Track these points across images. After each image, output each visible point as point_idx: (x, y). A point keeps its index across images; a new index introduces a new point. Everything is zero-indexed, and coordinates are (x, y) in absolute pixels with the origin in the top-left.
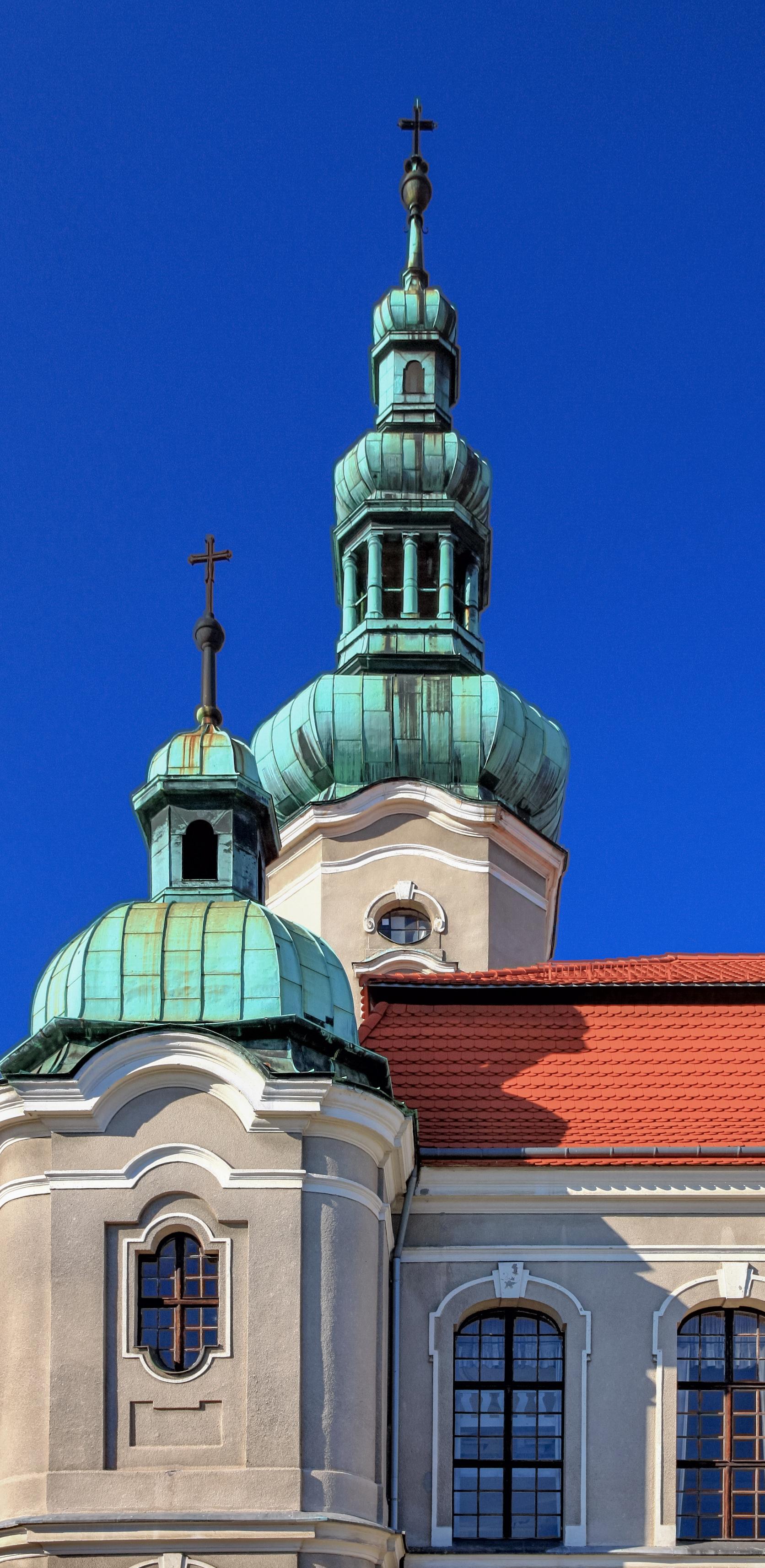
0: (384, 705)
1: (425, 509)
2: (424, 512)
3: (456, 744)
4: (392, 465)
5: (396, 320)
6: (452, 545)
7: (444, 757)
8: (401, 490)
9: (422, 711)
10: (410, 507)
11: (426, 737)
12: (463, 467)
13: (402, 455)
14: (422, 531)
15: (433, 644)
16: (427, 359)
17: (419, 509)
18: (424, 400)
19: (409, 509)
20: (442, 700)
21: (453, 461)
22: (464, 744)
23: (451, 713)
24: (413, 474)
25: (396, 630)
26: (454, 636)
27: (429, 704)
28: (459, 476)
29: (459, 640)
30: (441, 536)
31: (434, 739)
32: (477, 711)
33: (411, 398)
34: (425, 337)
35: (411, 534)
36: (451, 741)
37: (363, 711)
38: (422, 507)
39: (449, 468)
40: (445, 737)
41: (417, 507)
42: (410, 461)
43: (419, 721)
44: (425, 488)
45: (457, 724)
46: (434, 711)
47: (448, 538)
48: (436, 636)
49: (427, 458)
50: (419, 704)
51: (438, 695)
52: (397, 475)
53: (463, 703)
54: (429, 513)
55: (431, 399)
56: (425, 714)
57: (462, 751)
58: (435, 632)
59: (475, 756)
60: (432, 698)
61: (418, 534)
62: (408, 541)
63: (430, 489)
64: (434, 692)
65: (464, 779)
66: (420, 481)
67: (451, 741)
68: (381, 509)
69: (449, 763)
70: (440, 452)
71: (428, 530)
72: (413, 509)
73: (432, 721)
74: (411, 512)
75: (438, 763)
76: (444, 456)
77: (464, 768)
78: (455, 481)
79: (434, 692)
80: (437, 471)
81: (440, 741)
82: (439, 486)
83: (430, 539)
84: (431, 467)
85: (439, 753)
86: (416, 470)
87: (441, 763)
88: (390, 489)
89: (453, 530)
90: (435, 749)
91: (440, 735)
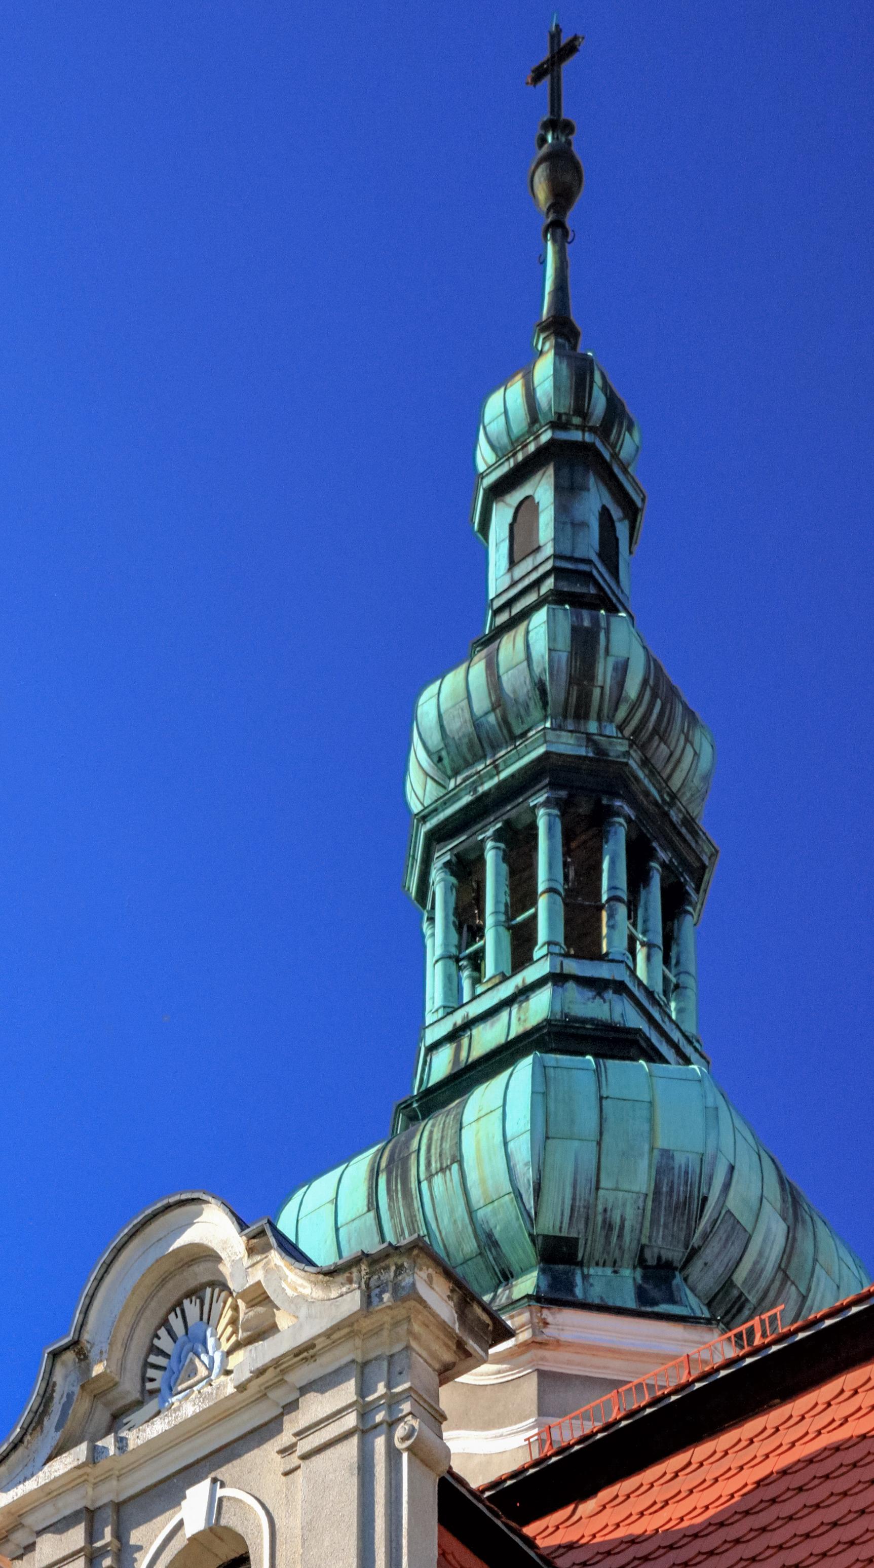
0: (365, 1202)
1: (503, 775)
2: (505, 780)
3: (480, 1214)
4: (458, 725)
5: (495, 443)
6: (556, 812)
7: (470, 1246)
8: (484, 757)
9: (419, 1182)
10: (482, 784)
11: (434, 1226)
12: (564, 656)
13: (469, 697)
14: (505, 817)
15: (523, 1018)
16: (543, 481)
17: (496, 780)
18: (540, 557)
19: (481, 790)
20: (447, 1146)
21: (543, 657)
22: (490, 1207)
23: (460, 1163)
24: (492, 718)
25: (469, 1024)
26: (555, 984)
27: (428, 1164)
28: (564, 677)
29: (571, 985)
30: (535, 806)
31: (445, 1221)
32: (499, 1138)
33: (519, 572)
34: (532, 448)
35: (490, 833)
36: (471, 1212)
37: (337, 1229)
38: (498, 773)
39: (541, 673)
40: (461, 1210)
41: (492, 777)
42: (481, 703)
43: (416, 1204)
44: (518, 731)
45: (472, 1177)
46: (437, 1173)
47: (547, 804)
48: (527, 999)
49: (504, 678)
50: (413, 1172)
51: (442, 1138)
52: (469, 735)
53: (478, 1133)
54: (513, 776)
55: (548, 550)
56: (424, 1185)
57: (492, 1223)
58: (525, 992)
59: (514, 1220)
60: (433, 1151)
61: (499, 825)
62: (489, 844)
63: (526, 727)
64: (436, 1136)
65: (516, 1268)
66: (505, 722)
67: (471, 1212)
68: (442, 816)
69: (481, 1254)
70: (522, 655)
71: (510, 811)
72: (487, 786)
73: (436, 1192)
74: (486, 794)
75: (465, 1262)
76: (529, 657)
77: (505, 1248)
78: (556, 693)
79: (436, 1136)
80: (525, 690)
81: (455, 1222)
82: (537, 713)
83: (526, 820)
84: (514, 692)
85: (460, 1244)
86: (493, 709)
87: (470, 1259)
88: (468, 765)
89: (553, 786)
90: (451, 1241)
91: (452, 1211)
